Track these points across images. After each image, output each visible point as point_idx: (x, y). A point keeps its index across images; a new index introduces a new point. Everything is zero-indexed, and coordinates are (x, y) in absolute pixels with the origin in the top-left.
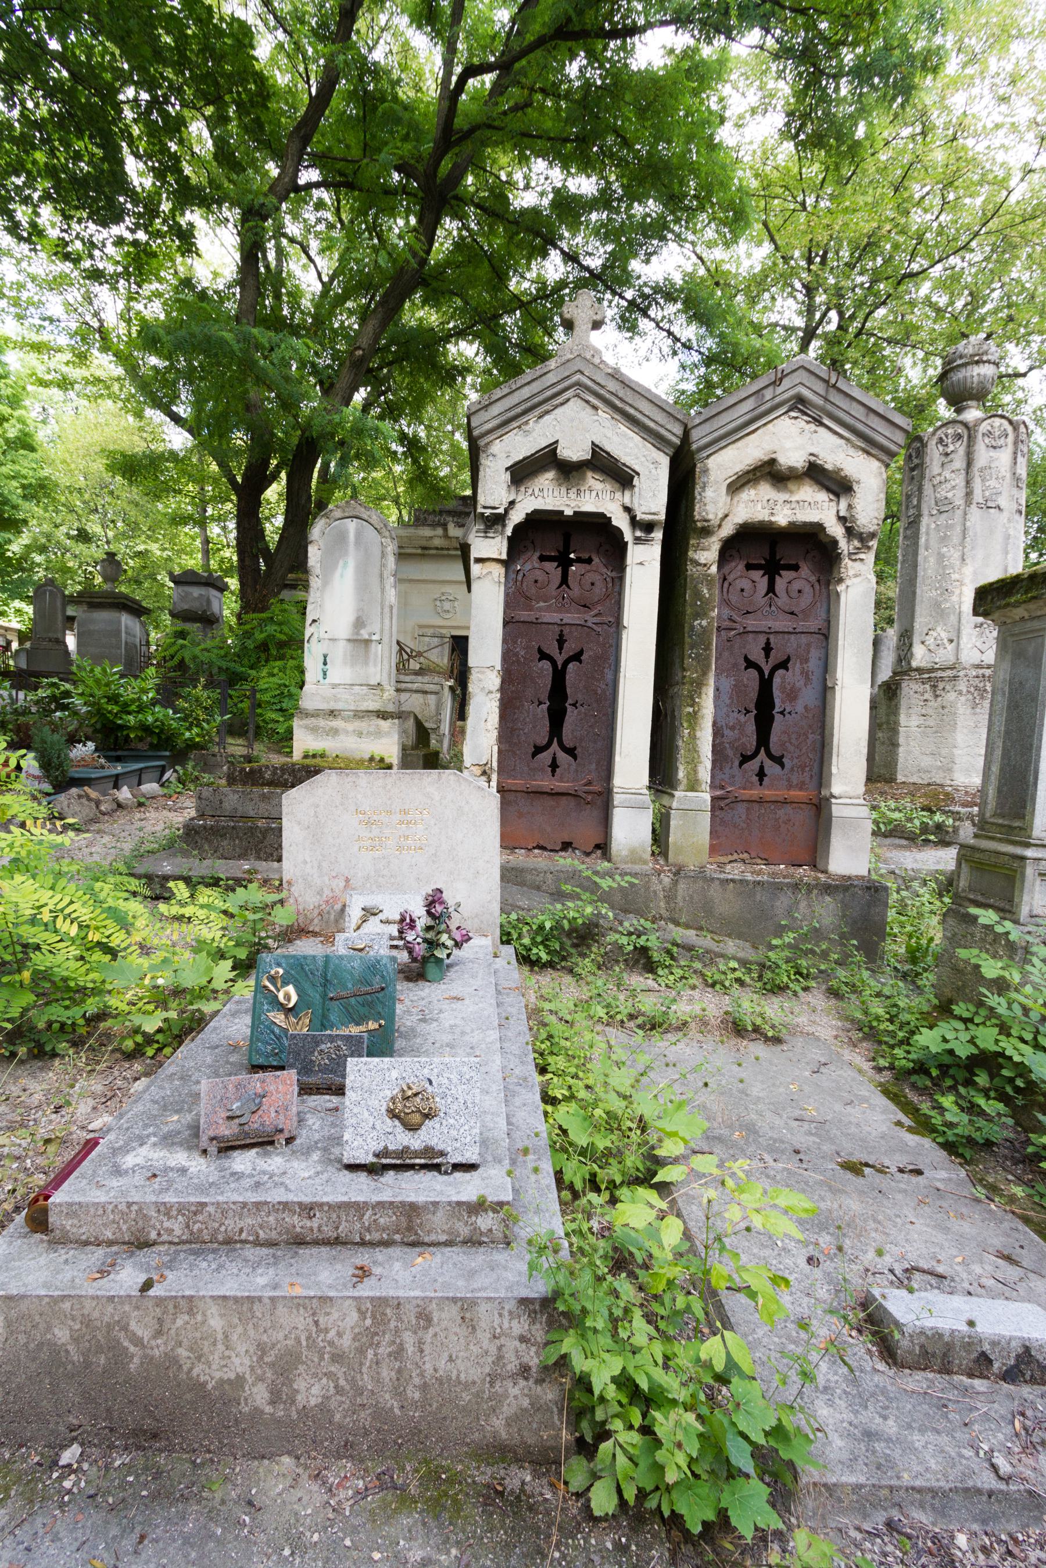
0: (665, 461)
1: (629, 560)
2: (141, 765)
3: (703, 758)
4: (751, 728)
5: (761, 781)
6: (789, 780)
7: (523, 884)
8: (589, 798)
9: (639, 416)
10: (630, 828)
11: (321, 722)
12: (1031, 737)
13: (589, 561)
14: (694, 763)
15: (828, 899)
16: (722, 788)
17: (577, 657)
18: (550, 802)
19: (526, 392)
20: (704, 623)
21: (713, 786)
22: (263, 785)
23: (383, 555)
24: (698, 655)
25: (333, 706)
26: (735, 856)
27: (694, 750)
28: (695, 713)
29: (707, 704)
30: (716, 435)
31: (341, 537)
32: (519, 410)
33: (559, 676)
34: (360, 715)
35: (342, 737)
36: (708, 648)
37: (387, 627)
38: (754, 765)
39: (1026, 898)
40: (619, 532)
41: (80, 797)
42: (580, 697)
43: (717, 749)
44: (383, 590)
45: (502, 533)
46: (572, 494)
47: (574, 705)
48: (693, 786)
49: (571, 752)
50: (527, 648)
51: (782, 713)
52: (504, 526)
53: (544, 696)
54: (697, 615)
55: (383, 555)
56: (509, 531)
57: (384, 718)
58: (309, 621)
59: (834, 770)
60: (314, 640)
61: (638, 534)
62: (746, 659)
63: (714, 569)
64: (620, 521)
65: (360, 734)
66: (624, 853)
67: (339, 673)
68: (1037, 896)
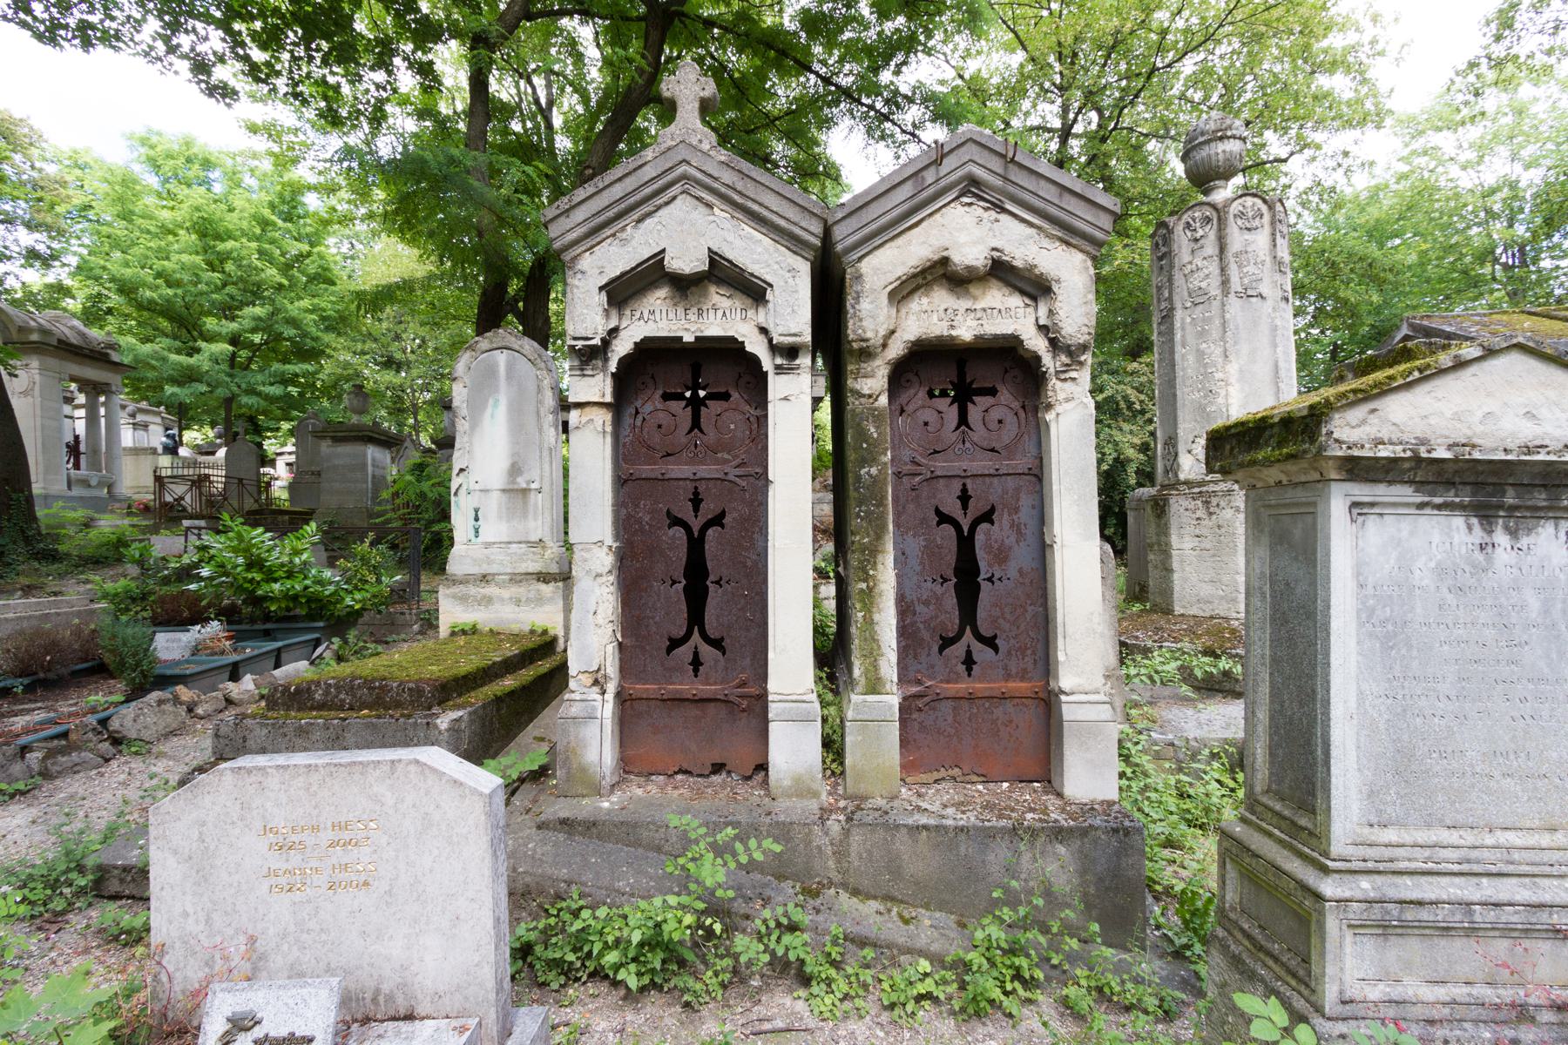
0: (804, 269)
1: (770, 397)
2: (280, 644)
3: (885, 649)
4: (951, 601)
5: (969, 670)
6: (1005, 668)
7: (637, 844)
8: (745, 703)
9: (765, 213)
10: (792, 748)
11: (473, 590)
12: (1312, 677)
13: (725, 396)
14: (873, 656)
15: (1061, 849)
16: (919, 682)
17: (718, 521)
18: (693, 711)
19: (617, 191)
20: (874, 471)
21: (903, 679)
22: (312, 708)
23: (539, 390)
24: (868, 513)
25: (485, 569)
26: (943, 773)
27: (872, 639)
28: (870, 589)
29: (886, 576)
30: (867, 230)
31: (491, 371)
32: (610, 214)
33: (696, 545)
34: (517, 579)
35: (497, 606)
36: (881, 503)
37: (547, 474)
38: (958, 650)
39: (1330, 970)
40: (754, 361)
41: (160, 702)
42: (725, 573)
43: (904, 631)
44: (540, 430)
45: (604, 369)
46: (692, 316)
47: (718, 583)
48: (874, 687)
49: (717, 644)
50: (651, 512)
51: (990, 579)
52: (606, 360)
53: (679, 573)
54: (863, 462)
55: (539, 390)
56: (613, 366)
57: (546, 582)
58: (455, 471)
59: (1061, 657)
60: (462, 492)
61: (779, 361)
62: (938, 512)
63: (883, 400)
64: (756, 346)
65: (518, 602)
66: (787, 783)
67: (494, 529)
68: (1349, 962)
